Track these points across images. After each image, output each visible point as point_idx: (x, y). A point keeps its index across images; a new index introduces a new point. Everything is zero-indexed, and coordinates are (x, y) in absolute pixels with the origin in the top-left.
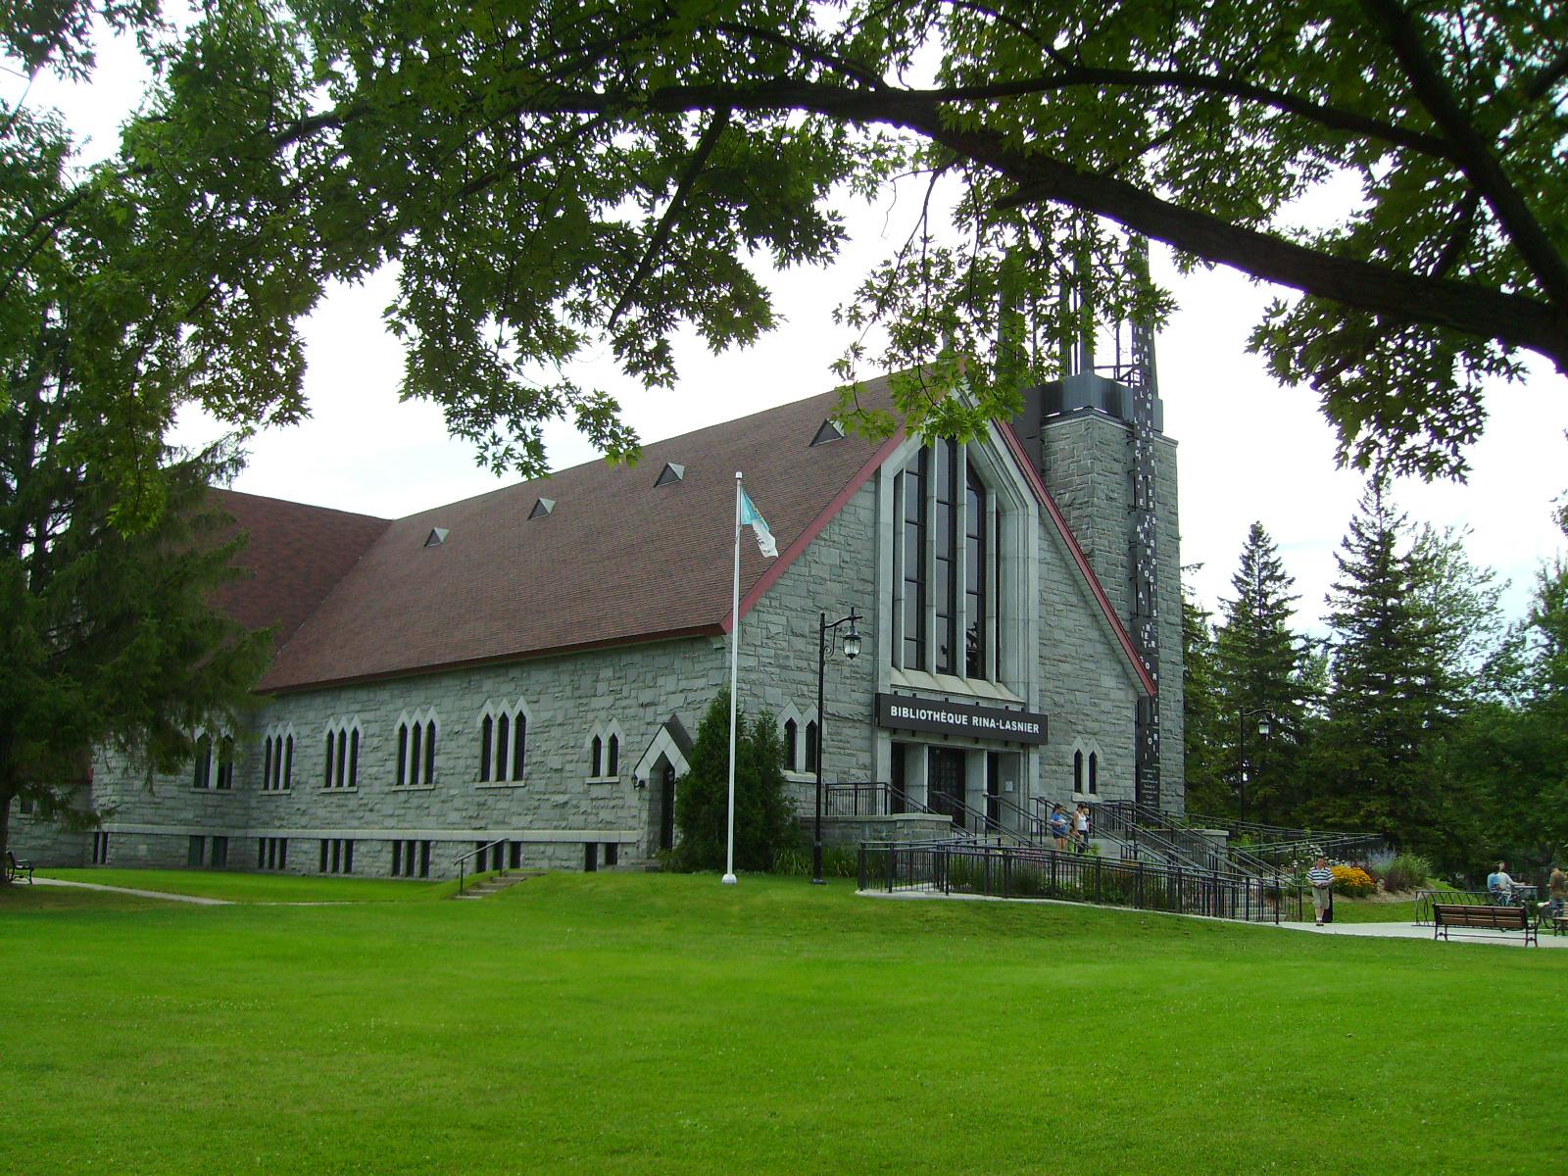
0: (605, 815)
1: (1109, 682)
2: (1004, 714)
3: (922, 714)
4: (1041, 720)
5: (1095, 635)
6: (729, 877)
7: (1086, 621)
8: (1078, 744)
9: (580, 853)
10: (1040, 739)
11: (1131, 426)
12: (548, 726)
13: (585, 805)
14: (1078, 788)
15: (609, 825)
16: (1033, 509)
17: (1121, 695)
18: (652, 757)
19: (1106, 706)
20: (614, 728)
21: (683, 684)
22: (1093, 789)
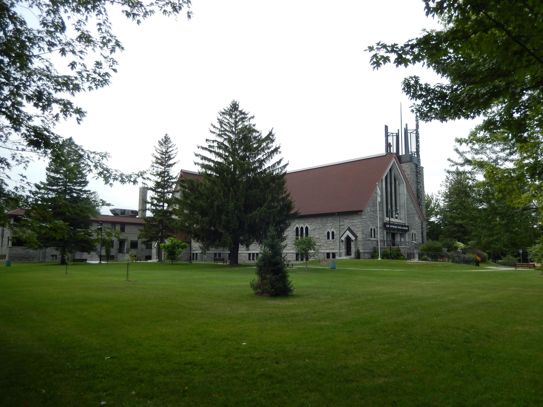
0: (331, 247)
1: (417, 218)
2: (402, 226)
3: (391, 226)
4: (408, 227)
5: (414, 209)
6: (379, 259)
7: (413, 206)
8: (413, 231)
9: (326, 255)
10: (408, 230)
11: (416, 164)
12: (315, 229)
13: (326, 245)
14: (371, 237)
15: (333, 249)
16: (405, 184)
17: (418, 221)
18: (345, 235)
19: (417, 223)
20: (333, 230)
21: (351, 221)
22: (374, 237)
